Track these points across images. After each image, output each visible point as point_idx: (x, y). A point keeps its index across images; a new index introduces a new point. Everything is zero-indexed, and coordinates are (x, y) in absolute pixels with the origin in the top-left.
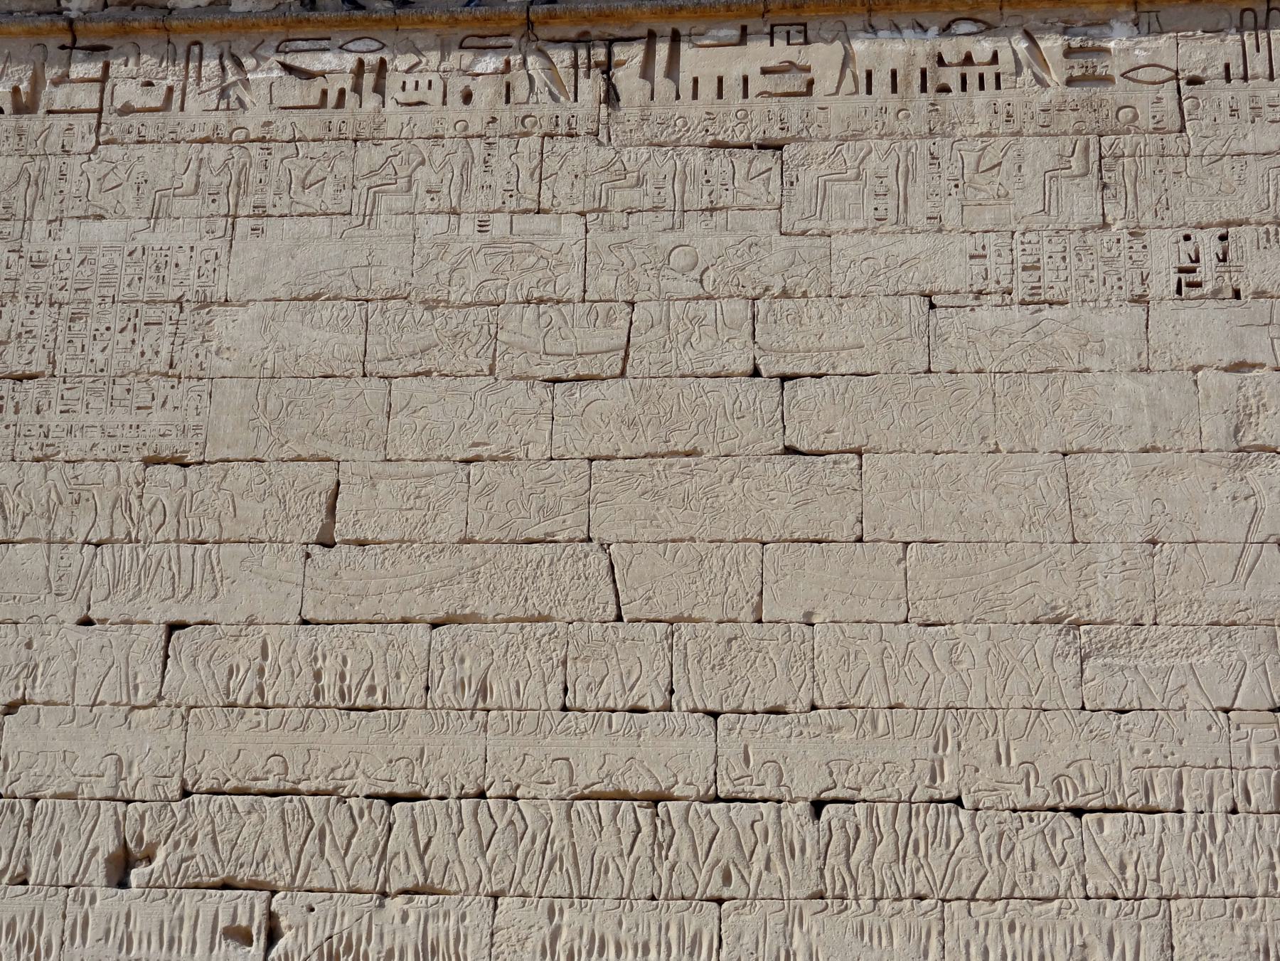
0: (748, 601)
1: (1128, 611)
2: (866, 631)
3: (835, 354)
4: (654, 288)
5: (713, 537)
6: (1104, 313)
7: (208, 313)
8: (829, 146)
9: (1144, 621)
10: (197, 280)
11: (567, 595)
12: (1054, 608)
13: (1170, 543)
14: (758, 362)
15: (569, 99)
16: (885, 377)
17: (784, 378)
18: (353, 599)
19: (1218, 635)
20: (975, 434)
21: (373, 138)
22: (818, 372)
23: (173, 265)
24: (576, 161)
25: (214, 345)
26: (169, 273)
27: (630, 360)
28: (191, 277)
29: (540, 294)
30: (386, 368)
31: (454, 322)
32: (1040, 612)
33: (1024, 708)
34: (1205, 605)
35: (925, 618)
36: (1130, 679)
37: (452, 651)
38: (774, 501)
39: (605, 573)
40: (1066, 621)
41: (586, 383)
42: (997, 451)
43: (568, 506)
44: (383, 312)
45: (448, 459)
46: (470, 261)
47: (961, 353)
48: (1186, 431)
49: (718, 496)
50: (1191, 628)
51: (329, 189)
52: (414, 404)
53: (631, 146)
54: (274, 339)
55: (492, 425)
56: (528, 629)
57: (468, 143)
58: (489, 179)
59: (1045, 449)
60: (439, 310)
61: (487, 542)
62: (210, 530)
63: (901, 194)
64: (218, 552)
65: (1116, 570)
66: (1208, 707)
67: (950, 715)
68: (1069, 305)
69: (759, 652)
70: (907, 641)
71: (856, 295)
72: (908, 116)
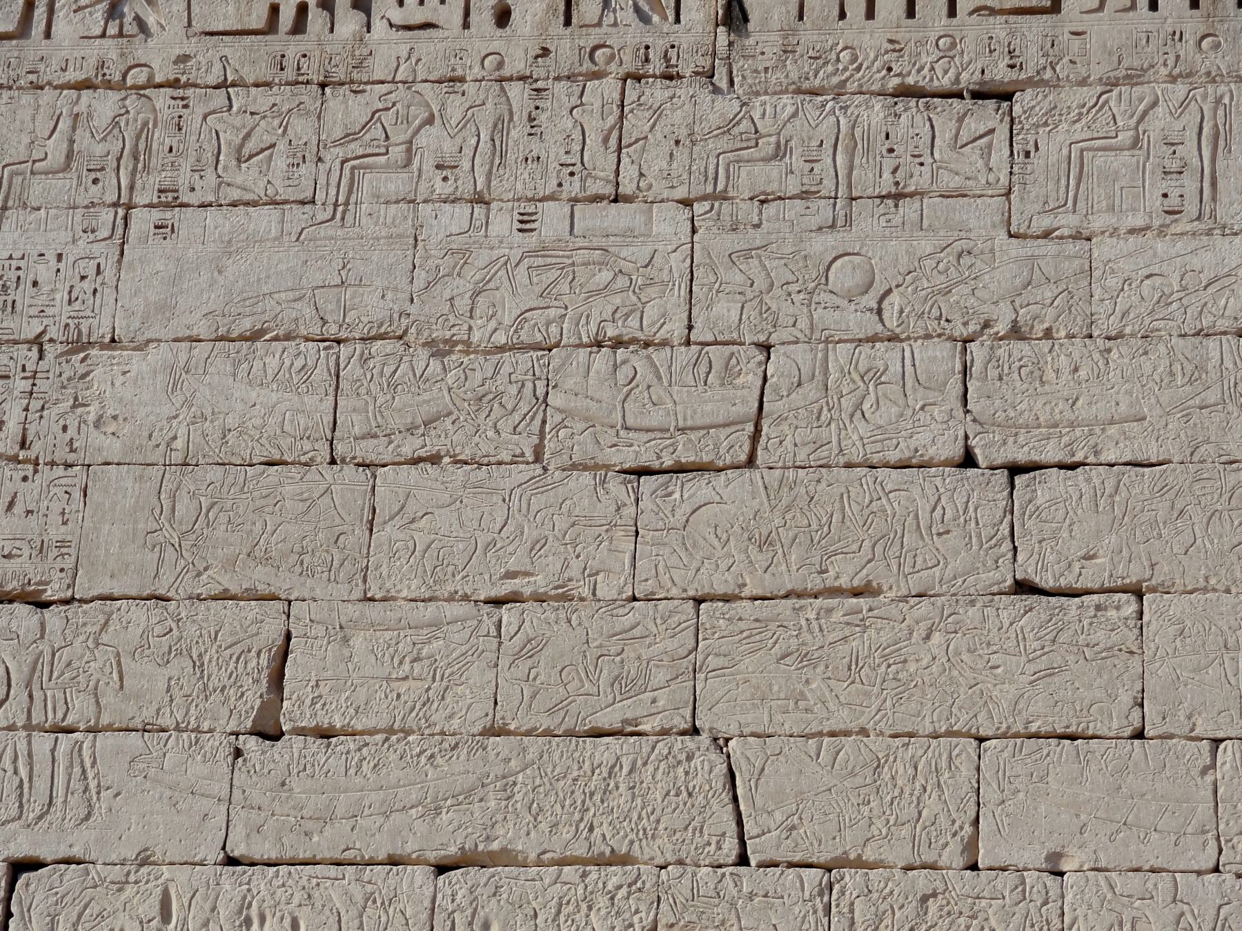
0: (954, 835)
2: (1150, 885)
3: (1097, 430)
4: (803, 323)
5: (899, 729)
7: (83, 360)
8: (1088, 94)
10: (66, 308)
11: (658, 821)
14: (973, 443)
15: (666, 18)
16: (1180, 468)
17: (1015, 470)
18: (309, 825)
21: (352, 82)
22: (1069, 460)
23: (29, 284)
24: (677, 118)
25: (92, 412)
26: (23, 296)
27: (763, 439)
28: (58, 303)
29: (616, 332)
30: (366, 450)
31: (478, 376)
37: (469, 912)
38: (999, 671)
39: (720, 785)
41: (690, 475)
43: (660, 677)
44: (364, 361)
45: (466, 598)
49: (905, 661)
51: (280, 163)
52: (412, 508)
53: (766, 93)
54: (188, 403)
55: (539, 544)
56: (594, 876)
57: (503, 89)
58: (536, 147)
60: (454, 357)
61: (528, 733)
62: (80, 710)
63: (1207, 171)
64: (94, 746)
69: (973, 917)
70: (1218, 902)
71: (1132, 335)
72: (1217, 46)
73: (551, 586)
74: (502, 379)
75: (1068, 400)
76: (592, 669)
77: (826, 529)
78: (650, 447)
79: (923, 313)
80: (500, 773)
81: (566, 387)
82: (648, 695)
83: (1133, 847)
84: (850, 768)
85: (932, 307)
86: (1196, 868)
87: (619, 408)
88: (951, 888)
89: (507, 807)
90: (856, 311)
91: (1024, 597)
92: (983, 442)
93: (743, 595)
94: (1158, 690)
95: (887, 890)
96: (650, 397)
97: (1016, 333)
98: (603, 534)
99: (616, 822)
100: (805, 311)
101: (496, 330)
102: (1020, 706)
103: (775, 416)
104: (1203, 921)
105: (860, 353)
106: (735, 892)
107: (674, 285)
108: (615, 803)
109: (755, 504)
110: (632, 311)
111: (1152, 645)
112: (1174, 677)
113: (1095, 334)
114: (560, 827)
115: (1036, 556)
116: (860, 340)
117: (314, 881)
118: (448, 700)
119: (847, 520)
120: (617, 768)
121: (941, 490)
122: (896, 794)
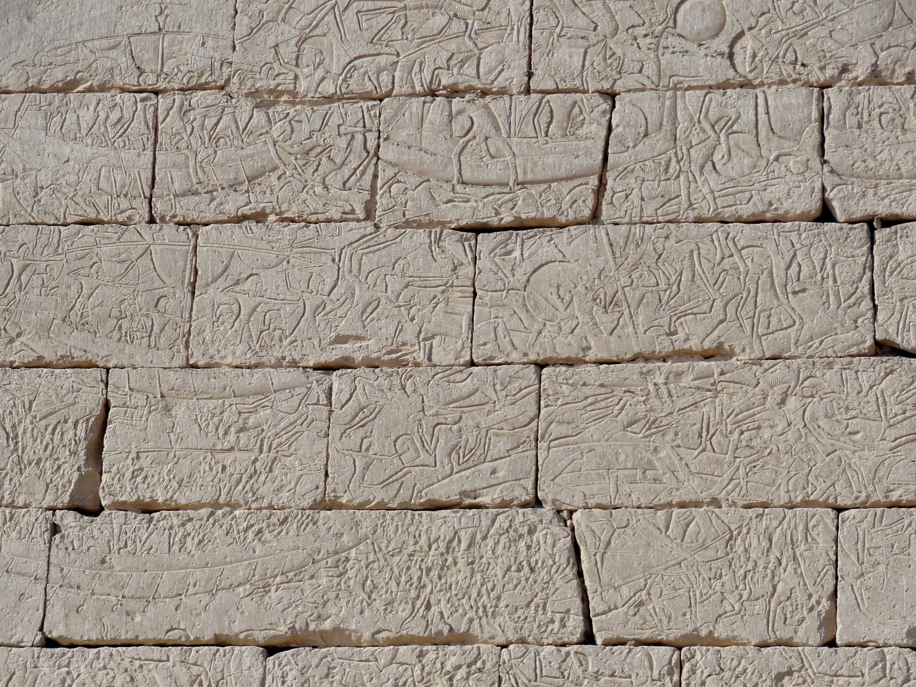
0: (811, 609)
4: (650, 69)
5: (753, 499)
11: (499, 598)
14: (830, 195)
17: (872, 224)
18: (131, 605)
27: (608, 194)
30: (188, 208)
31: (305, 128)
38: (858, 437)
39: (564, 560)
41: (531, 232)
43: (499, 446)
44: (184, 113)
45: (294, 364)
46: (333, 24)
49: (759, 428)
52: (237, 268)
56: (431, 656)
60: (279, 108)
61: (361, 507)
73: (384, 351)
74: (330, 131)
76: (428, 438)
77: (675, 288)
78: (488, 202)
79: (777, 57)
80: (331, 549)
81: (399, 139)
82: (488, 465)
84: (700, 541)
85: (787, 50)
87: (455, 161)
88: (807, 666)
89: (339, 584)
90: (706, 55)
91: (885, 358)
92: (841, 195)
93: (587, 359)
95: (740, 669)
96: (488, 150)
97: (876, 77)
98: (439, 296)
99: (455, 599)
100: (652, 56)
101: (323, 79)
102: (881, 473)
103: (621, 169)
105: (711, 100)
106: (579, 672)
107: (512, 29)
108: (454, 579)
109: (600, 262)
110: (468, 58)
114: (396, 604)
115: (897, 315)
116: (711, 87)
117: (137, 663)
118: (276, 472)
119: (697, 278)
120: (455, 543)
121: (797, 246)
122: (750, 567)
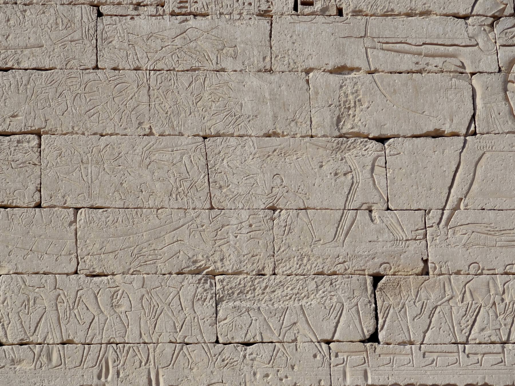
1: (253, 264)
2: (43, 281)
3: (19, 51)
6: (237, 24)
9: (266, 271)
12: (195, 262)
13: (287, 209)
16: (60, 72)
19: (322, 282)
20: (134, 119)
22: (5, 66)
32: (184, 265)
33: (171, 342)
34: (313, 259)
35: (91, 270)
36: (254, 318)
40: (205, 272)
42: (151, 134)
47: (123, 53)
48: (300, 120)
50: (302, 277)
59: (190, 133)
65: (244, 231)
66: (314, 340)
67: (111, 350)
68: (210, 17)
70: (77, 289)
71: (37, 3)
75: (4, 36)
83: (35, 262)
86: (66, 272)
94: (48, 183)
104: (69, 298)
111: (45, 161)
112: (56, 177)
113: (18, 2)
